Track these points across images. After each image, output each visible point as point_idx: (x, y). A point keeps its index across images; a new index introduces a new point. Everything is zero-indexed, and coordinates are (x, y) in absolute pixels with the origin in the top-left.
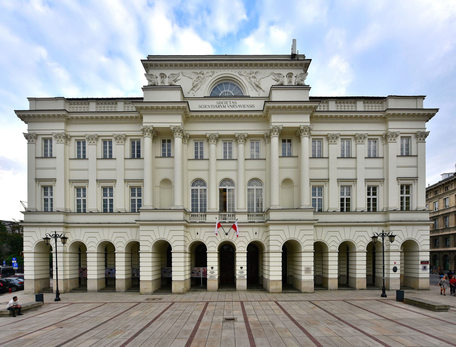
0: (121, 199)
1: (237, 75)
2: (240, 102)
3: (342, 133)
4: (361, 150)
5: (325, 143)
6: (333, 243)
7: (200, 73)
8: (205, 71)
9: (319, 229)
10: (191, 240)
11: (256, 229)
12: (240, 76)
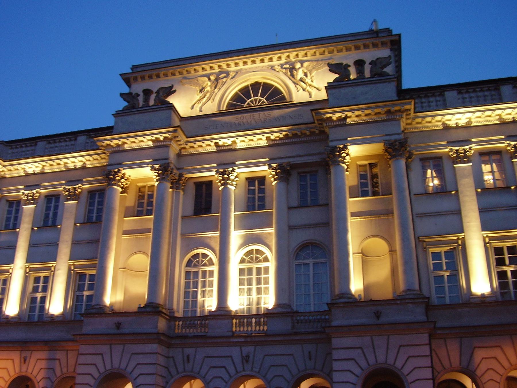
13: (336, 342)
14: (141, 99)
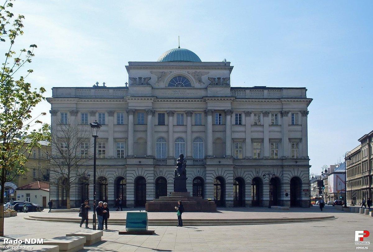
0: (111, 151)
1: (186, 73)
2: (188, 91)
3: (252, 110)
4: (267, 121)
5: (243, 116)
6: (248, 178)
7: (162, 73)
8: (166, 71)
9: (239, 170)
10: (156, 175)
11: (199, 169)
12: (188, 74)
13: (208, 169)
14: (138, 80)
